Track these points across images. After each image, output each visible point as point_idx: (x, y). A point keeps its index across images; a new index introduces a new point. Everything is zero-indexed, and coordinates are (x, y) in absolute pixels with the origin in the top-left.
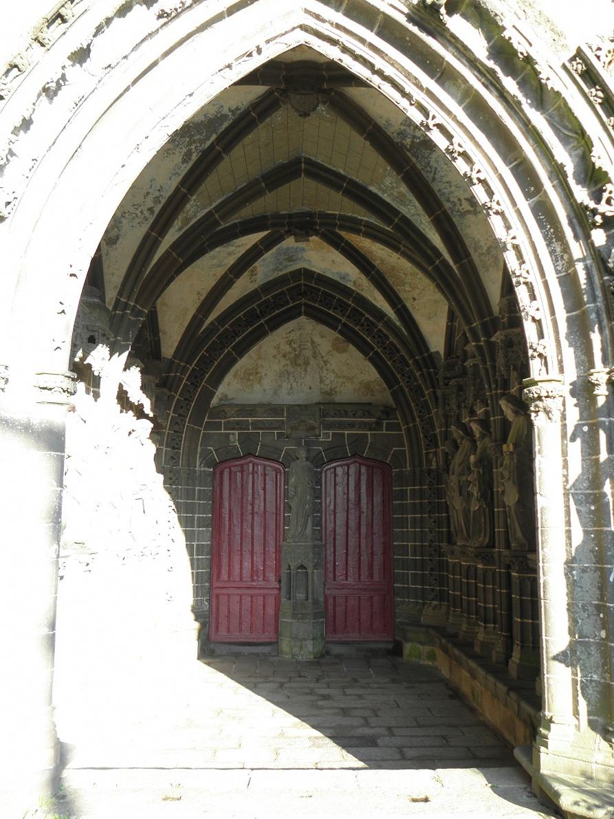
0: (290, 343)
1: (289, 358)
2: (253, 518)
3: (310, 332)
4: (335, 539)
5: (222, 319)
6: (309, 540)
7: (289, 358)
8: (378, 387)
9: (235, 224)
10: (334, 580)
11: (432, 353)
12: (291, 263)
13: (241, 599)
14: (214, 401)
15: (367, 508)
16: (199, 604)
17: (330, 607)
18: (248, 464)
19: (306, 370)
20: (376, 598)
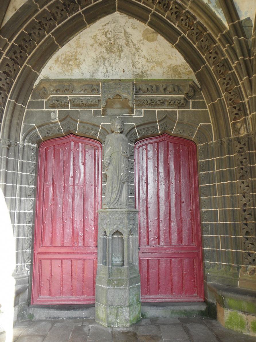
1: (105, 47)
2: (74, 188)
4: (147, 208)
6: (124, 206)
7: (105, 47)
8: (184, 71)
10: (148, 244)
11: (242, 21)
13: (62, 263)
15: (175, 179)
16: (19, 270)
17: (145, 270)
20: (186, 261)
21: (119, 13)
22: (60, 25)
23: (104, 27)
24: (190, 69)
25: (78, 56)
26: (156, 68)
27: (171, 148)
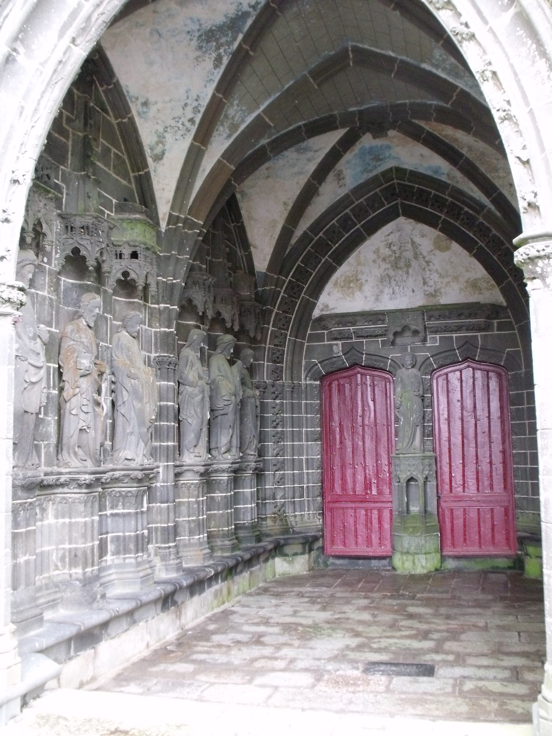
0: (389, 246)
2: (363, 429)
3: (410, 232)
5: (316, 227)
6: (418, 452)
7: (390, 262)
9: (300, 127)
12: (379, 163)
13: (355, 512)
14: (316, 313)
16: (312, 518)
18: (355, 375)
19: (407, 273)
21: (404, 218)
22: (337, 245)
23: (387, 237)
24: (493, 282)
25: (360, 276)
26: (452, 284)
27: (478, 374)
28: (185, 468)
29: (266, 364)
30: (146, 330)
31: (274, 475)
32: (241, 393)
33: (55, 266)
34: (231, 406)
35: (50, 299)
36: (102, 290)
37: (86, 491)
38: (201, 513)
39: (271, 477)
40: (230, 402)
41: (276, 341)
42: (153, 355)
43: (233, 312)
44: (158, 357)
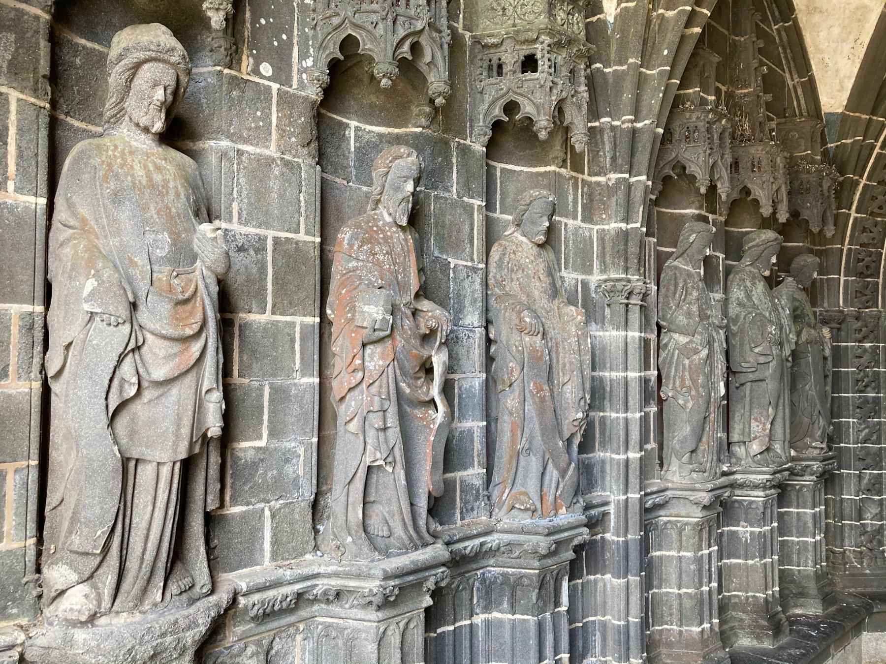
28: (669, 493)
29: (842, 279)
30: (577, 229)
31: (860, 477)
32: (793, 337)
33: (302, 86)
34: (774, 362)
35: (287, 163)
36: (453, 145)
37: (380, 615)
38: (705, 580)
39: (854, 482)
40: (771, 358)
41: (865, 238)
42: (595, 278)
43: (775, 187)
44: (606, 281)
